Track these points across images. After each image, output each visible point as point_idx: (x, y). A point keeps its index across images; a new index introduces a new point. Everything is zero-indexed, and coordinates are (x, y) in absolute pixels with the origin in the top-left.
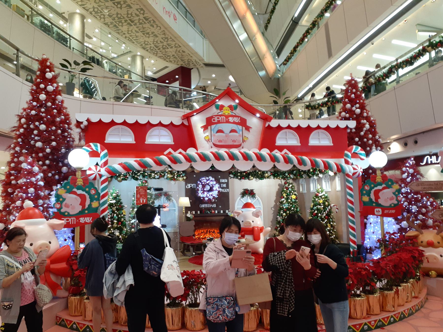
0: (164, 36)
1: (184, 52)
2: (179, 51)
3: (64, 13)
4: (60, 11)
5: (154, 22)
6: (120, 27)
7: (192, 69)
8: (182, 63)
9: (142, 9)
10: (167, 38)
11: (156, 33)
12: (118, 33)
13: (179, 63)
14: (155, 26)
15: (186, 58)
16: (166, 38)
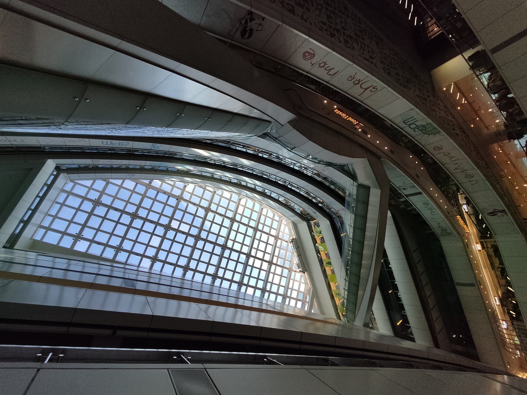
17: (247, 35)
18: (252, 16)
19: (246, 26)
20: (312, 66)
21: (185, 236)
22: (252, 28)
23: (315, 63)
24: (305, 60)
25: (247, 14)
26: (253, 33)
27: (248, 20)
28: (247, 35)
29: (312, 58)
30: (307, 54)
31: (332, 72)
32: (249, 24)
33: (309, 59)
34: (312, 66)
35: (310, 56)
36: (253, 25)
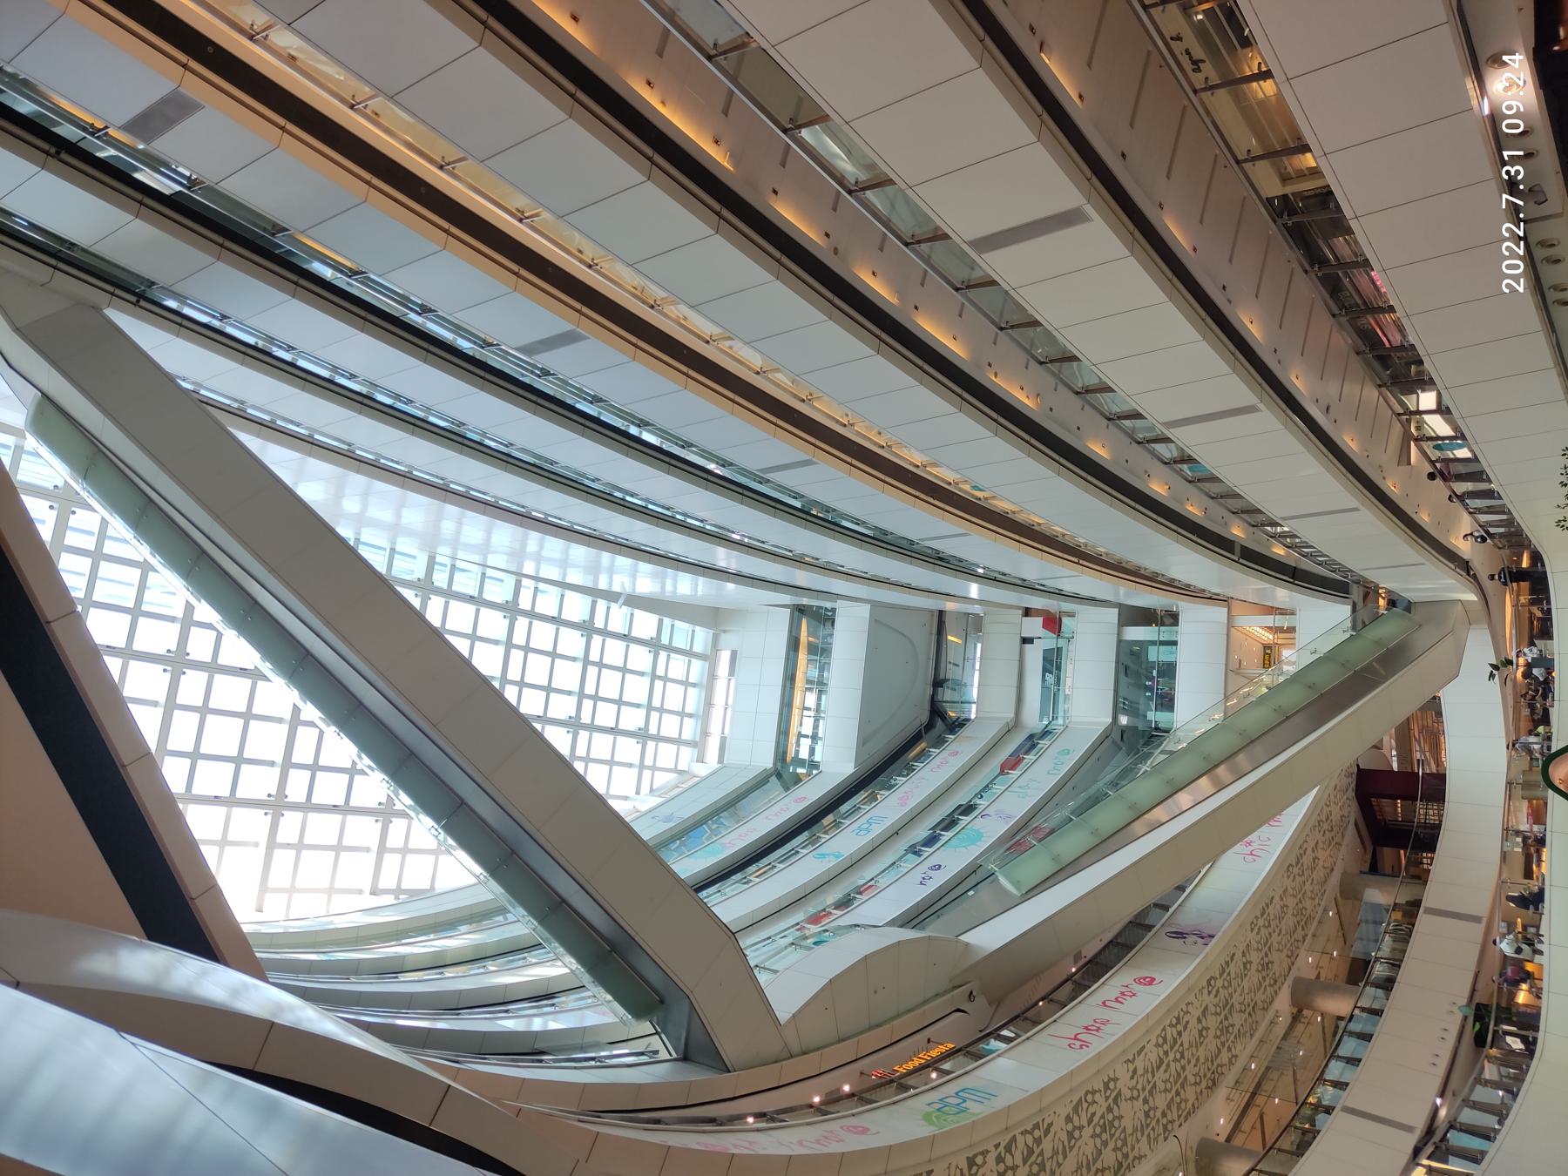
0: (1317, 829)
1: (1336, 786)
2: (1335, 797)
4: (1290, 1021)
5: (1301, 847)
6: (1308, 912)
7: (1358, 766)
8: (1350, 790)
9: (1288, 870)
10: (1319, 822)
11: (1313, 844)
12: (1314, 918)
13: (1351, 798)
14: (1306, 845)
15: (1345, 781)
16: (1319, 825)
21: (136, 647)
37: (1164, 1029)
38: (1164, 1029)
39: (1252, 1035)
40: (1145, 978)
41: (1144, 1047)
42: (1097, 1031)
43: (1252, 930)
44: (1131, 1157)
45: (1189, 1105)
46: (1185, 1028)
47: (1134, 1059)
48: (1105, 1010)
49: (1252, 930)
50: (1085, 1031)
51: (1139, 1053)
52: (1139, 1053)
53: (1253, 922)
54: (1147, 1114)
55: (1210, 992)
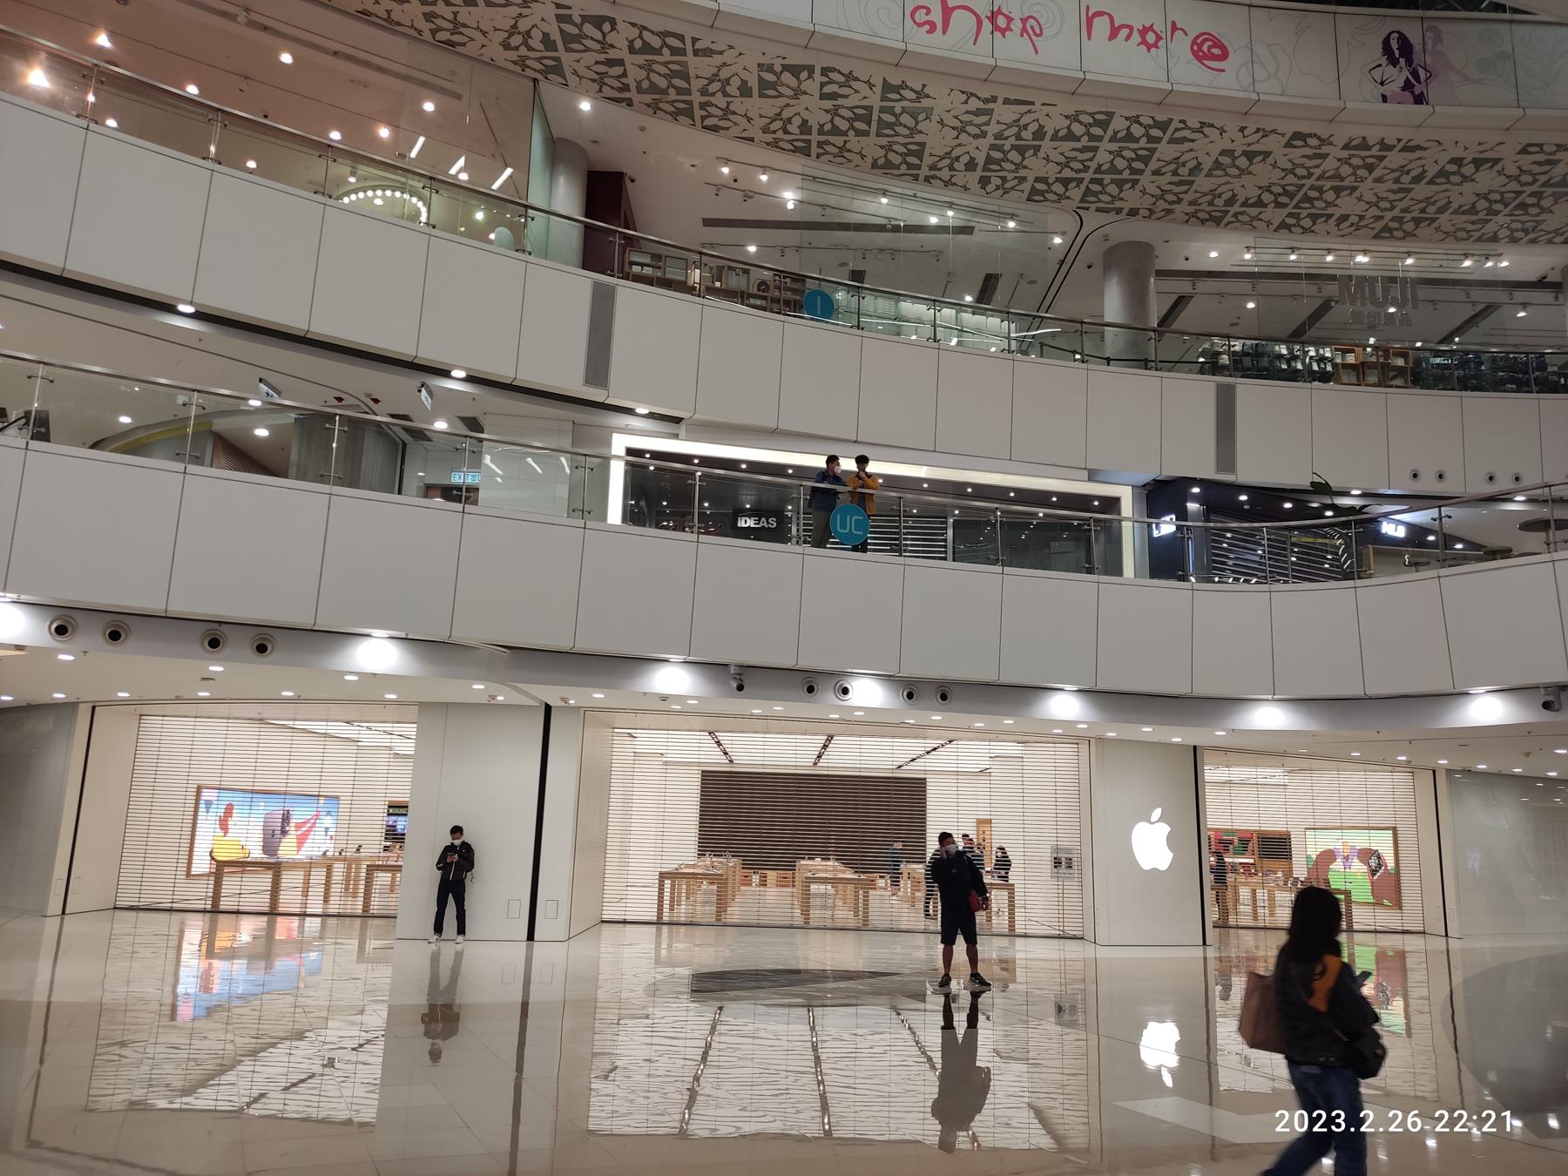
3: (1545, 278)
4: (1533, 277)
17: (1394, 45)
18: (1413, 93)
19: (1410, 67)
20: (1174, 24)
22: (1395, 67)
23: (1172, 35)
24: (1210, 34)
25: (1426, 94)
26: (1384, 55)
27: (1415, 83)
28: (1394, 45)
29: (1195, 47)
30: (1216, 51)
31: (1101, 26)
32: (1406, 74)
33: (1199, 41)
34: (1174, 24)
35: (1205, 48)
36: (1398, 75)
37: (1111, 115)
38: (1111, 115)
39: (1377, 237)
40: (1217, 43)
41: (1033, 103)
42: (996, 28)
43: (1524, 151)
44: (924, 171)
45: (1127, 206)
46: (1172, 141)
47: (994, 99)
48: (1073, 21)
49: (1524, 151)
50: (984, 12)
51: (1007, 101)
52: (1007, 101)
53: (1541, 146)
54: (989, 160)
55: (1288, 145)
